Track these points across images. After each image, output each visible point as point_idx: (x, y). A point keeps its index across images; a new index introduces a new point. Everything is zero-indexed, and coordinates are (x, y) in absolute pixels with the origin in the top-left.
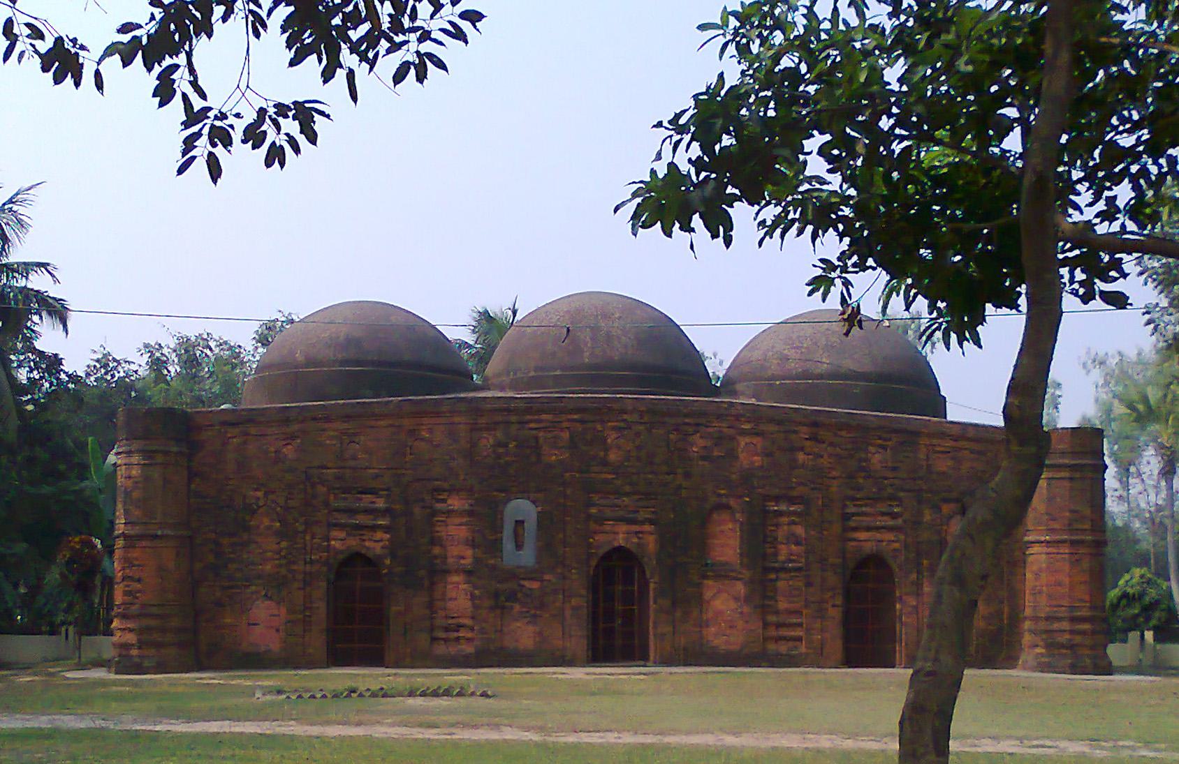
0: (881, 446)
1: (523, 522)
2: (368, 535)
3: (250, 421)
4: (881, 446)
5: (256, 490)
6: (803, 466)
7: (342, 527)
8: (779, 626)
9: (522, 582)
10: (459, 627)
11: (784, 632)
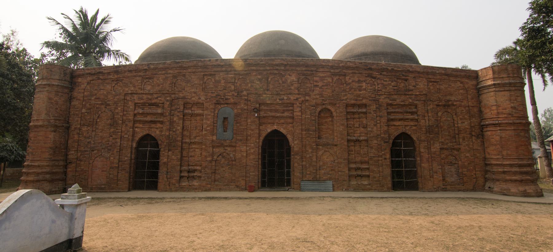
0: (403, 79)
1: (227, 118)
2: (153, 125)
3: (100, 73)
4: (403, 79)
5: (102, 104)
6: (365, 89)
7: (140, 122)
8: (357, 169)
9: (226, 148)
10: (194, 171)
11: (359, 173)
